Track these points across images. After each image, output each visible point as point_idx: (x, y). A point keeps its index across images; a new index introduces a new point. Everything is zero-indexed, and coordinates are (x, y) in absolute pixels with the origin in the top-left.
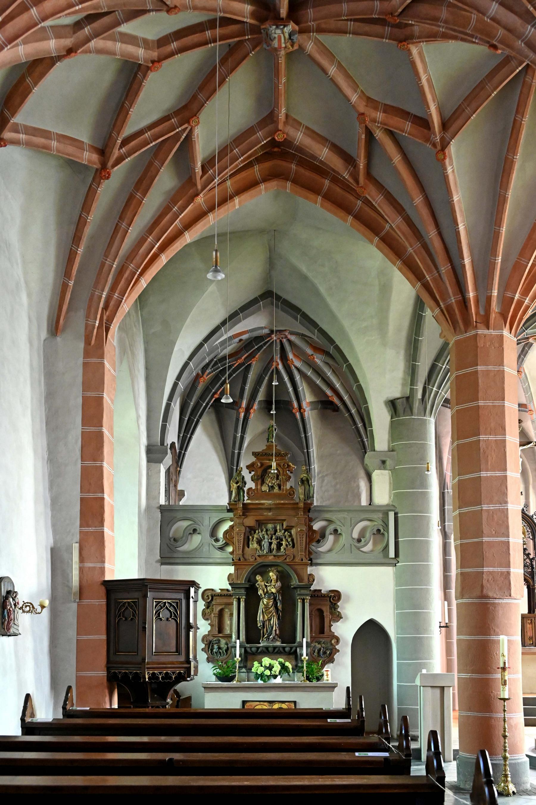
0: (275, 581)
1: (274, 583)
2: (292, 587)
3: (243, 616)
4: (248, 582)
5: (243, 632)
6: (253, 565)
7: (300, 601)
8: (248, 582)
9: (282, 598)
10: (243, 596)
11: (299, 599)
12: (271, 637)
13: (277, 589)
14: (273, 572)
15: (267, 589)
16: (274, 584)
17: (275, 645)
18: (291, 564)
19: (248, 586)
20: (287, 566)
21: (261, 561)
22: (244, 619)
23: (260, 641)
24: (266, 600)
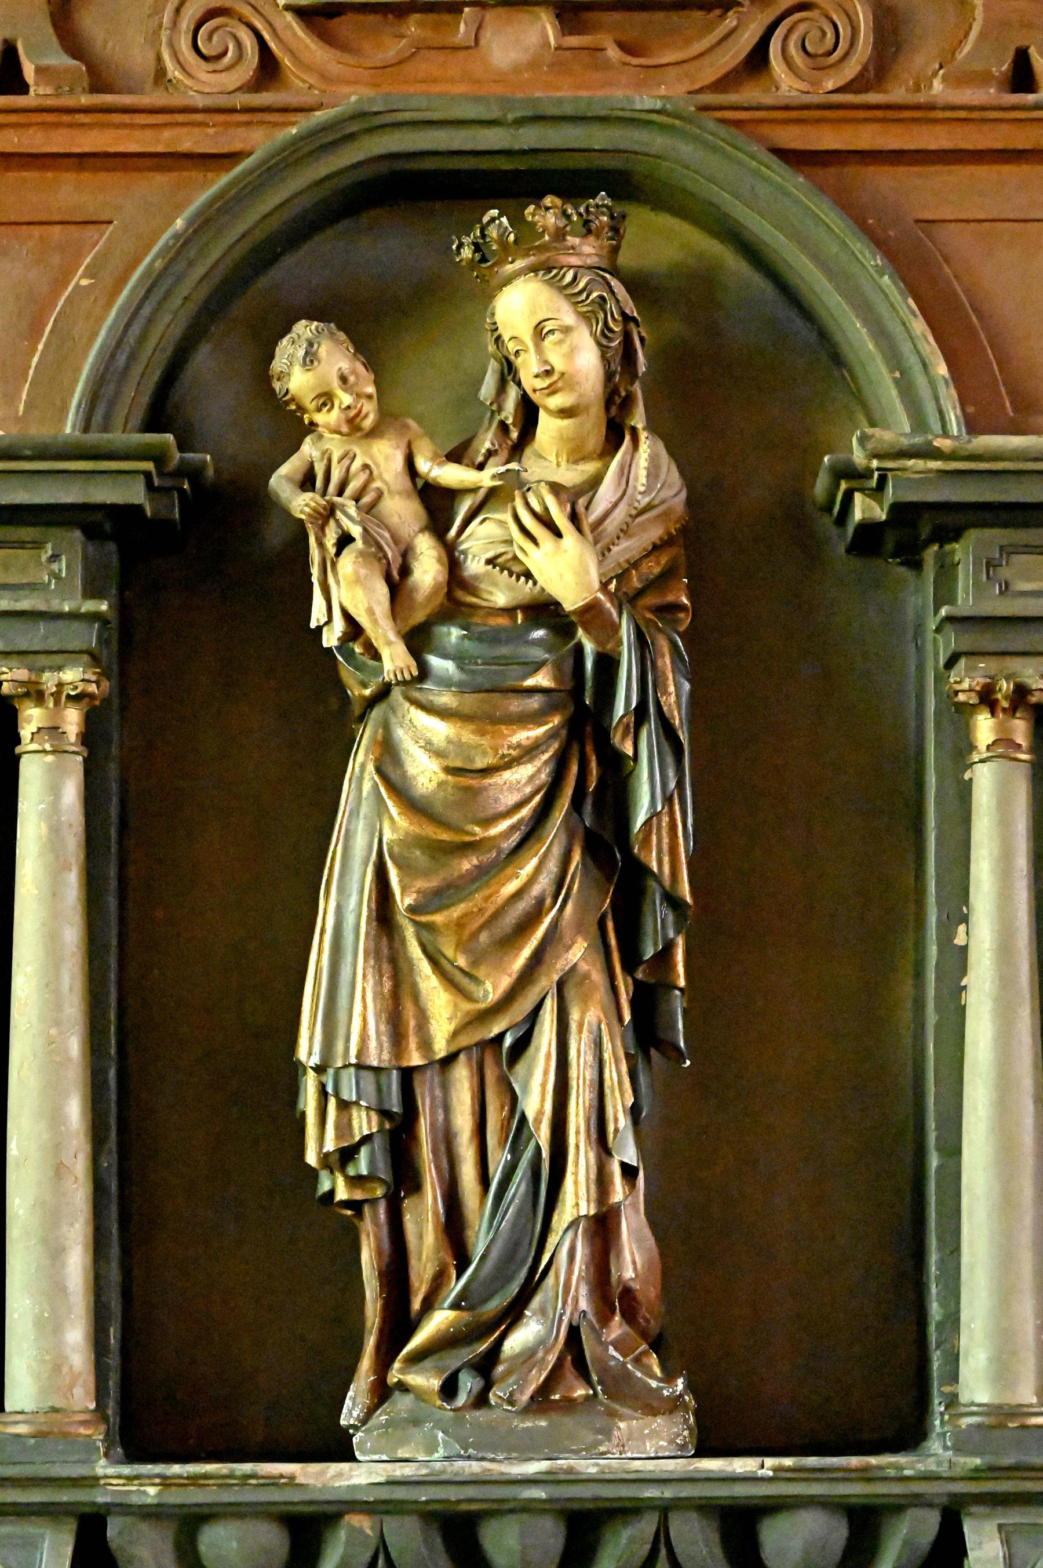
0: (595, 439)
1: (577, 456)
2: (863, 509)
3: (51, 985)
4: (154, 421)
5: (56, 1253)
6: (233, 157)
7: (1004, 742)
8: (154, 421)
9: (696, 704)
10: (65, 655)
11: (987, 698)
12: (516, 1342)
13: (625, 550)
14: (544, 268)
15: (453, 563)
16: (571, 476)
17: (589, 1467)
18: (828, 139)
19: (135, 494)
20: (794, 182)
21: (353, 97)
22: (75, 1046)
23: (350, 1413)
24: (440, 730)
